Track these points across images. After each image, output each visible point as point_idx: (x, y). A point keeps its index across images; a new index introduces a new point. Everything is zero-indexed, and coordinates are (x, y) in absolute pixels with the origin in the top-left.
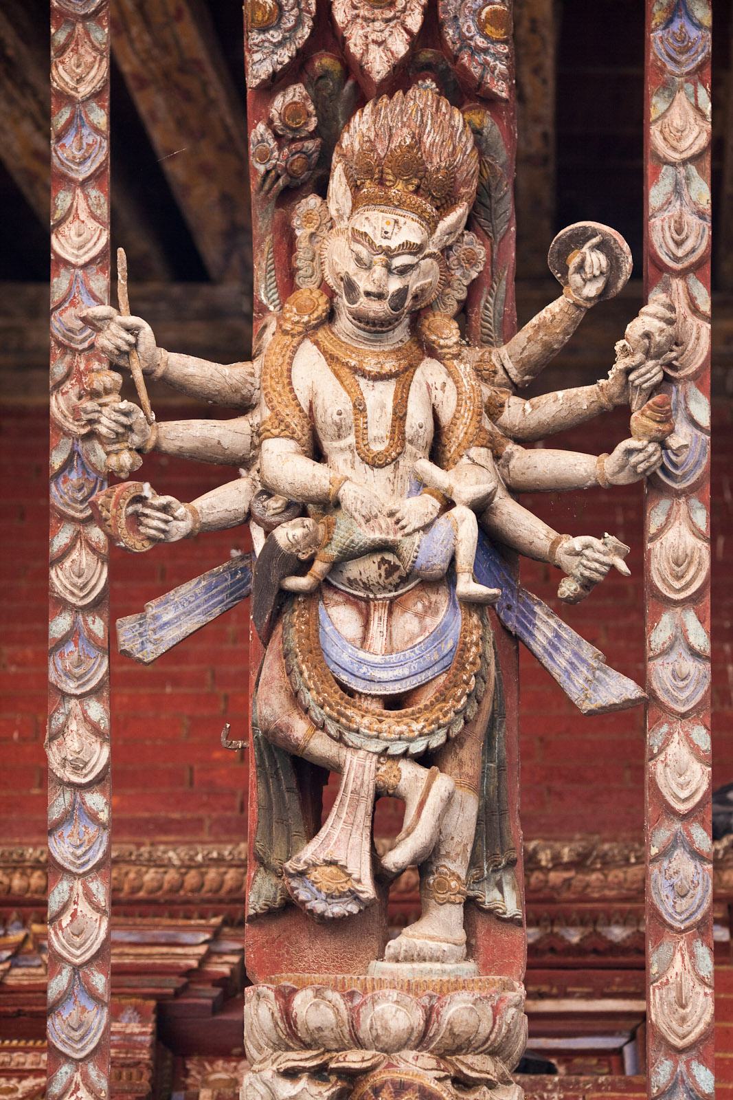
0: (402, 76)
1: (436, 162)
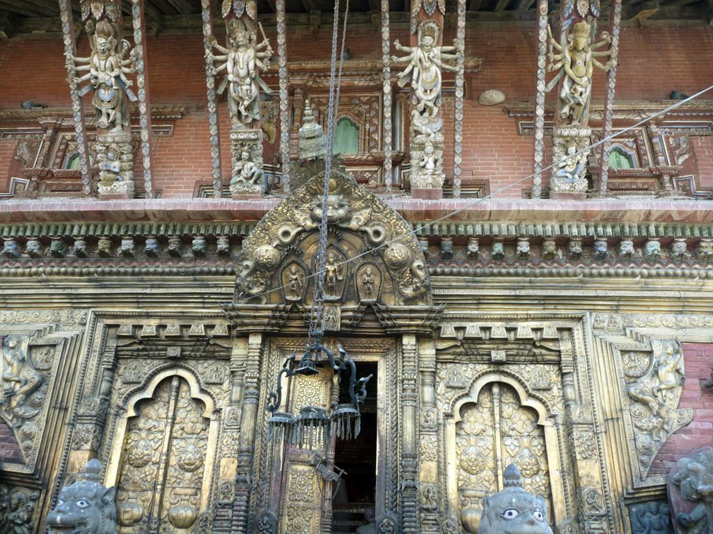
0: (101, 19)
1: (106, 31)
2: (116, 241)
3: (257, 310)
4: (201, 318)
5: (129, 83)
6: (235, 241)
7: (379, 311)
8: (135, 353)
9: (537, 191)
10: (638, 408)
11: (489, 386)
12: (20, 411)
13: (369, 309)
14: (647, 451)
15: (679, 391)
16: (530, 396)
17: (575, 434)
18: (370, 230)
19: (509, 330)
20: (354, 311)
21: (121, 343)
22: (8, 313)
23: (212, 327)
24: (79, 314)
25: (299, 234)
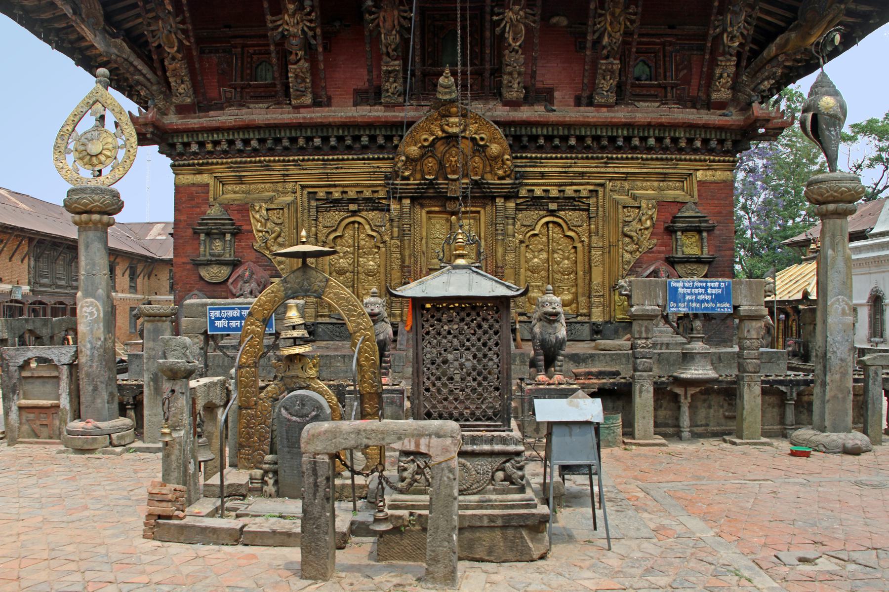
2: (309, 139)
3: (408, 185)
5: (311, 33)
6: (389, 138)
7: (483, 183)
9: (584, 101)
10: (627, 240)
11: (547, 223)
13: (476, 183)
14: (628, 262)
15: (651, 230)
16: (570, 229)
17: (593, 252)
18: (477, 137)
19: (560, 191)
20: (467, 184)
23: (377, 192)
25: (434, 140)
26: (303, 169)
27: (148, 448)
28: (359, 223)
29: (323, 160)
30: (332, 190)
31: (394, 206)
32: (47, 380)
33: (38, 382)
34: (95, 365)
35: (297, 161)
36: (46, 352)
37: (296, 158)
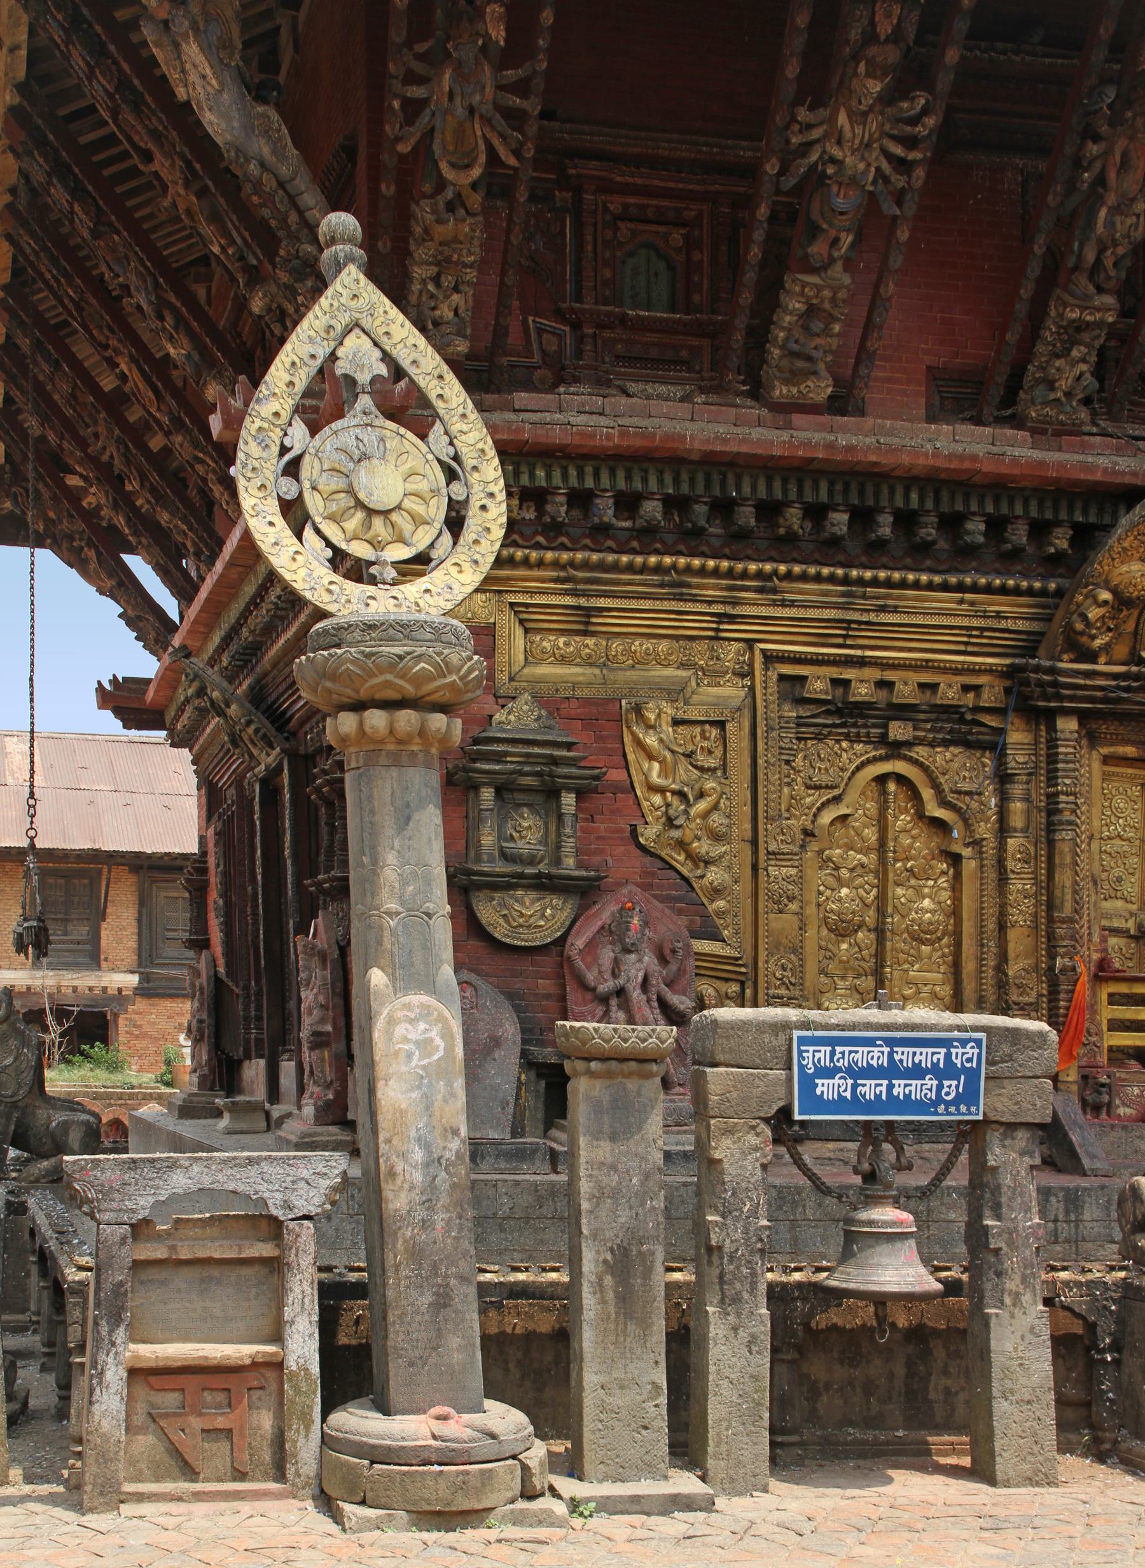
4: (956, 671)
8: (825, 731)
12: (703, 847)
21: (805, 711)
22: (590, 641)
23: (977, 689)
24: (730, 653)
26: (784, 604)
27: (635, 1499)
28: (900, 779)
29: (846, 581)
30: (848, 674)
31: (1017, 736)
32: (215, 1272)
33: (182, 1279)
34: (440, 1218)
35: (768, 577)
36: (242, 1174)
37: (768, 567)
